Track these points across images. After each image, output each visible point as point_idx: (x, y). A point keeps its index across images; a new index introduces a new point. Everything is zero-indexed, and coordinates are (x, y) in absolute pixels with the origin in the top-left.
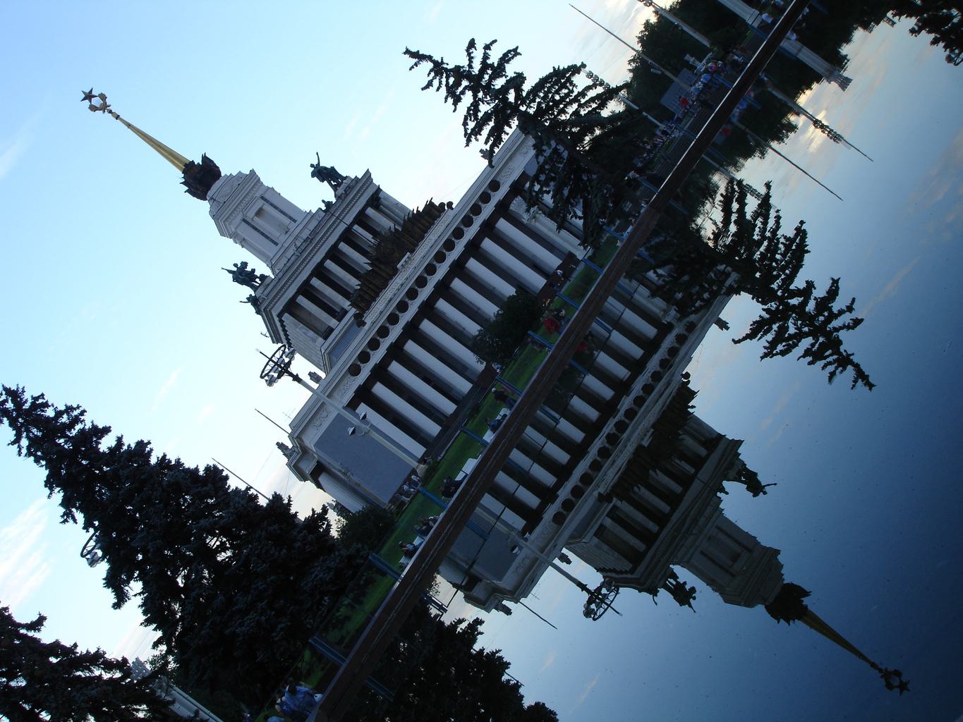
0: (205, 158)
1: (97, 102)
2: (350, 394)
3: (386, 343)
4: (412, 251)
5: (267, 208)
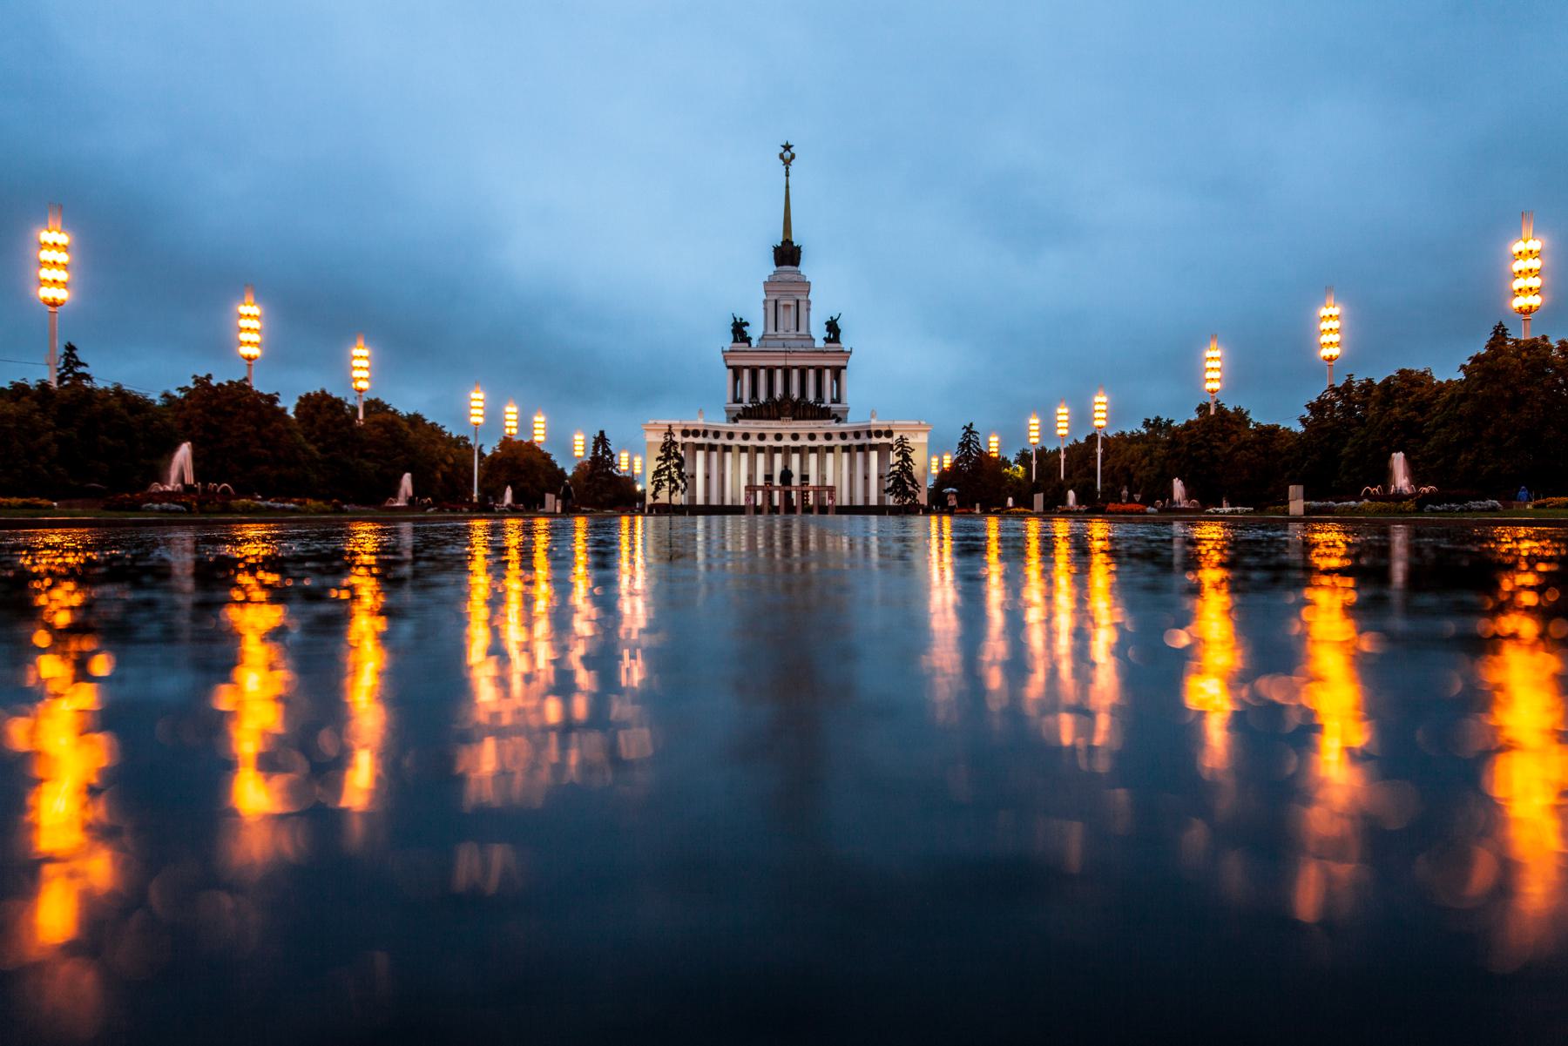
0: (798, 249)
1: (787, 155)
5: (793, 310)
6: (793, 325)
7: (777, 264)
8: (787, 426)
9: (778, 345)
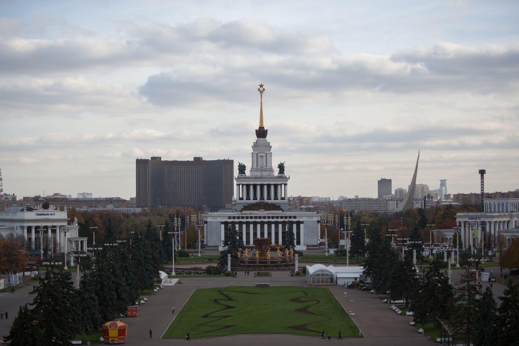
2: (224, 220)
3: (241, 220)
4: (266, 210)
5: (264, 158)
6: (265, 165)
7: (258, 137)
8: (262, 213)
9: (258, 174)
